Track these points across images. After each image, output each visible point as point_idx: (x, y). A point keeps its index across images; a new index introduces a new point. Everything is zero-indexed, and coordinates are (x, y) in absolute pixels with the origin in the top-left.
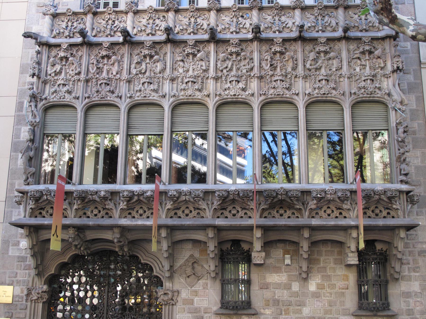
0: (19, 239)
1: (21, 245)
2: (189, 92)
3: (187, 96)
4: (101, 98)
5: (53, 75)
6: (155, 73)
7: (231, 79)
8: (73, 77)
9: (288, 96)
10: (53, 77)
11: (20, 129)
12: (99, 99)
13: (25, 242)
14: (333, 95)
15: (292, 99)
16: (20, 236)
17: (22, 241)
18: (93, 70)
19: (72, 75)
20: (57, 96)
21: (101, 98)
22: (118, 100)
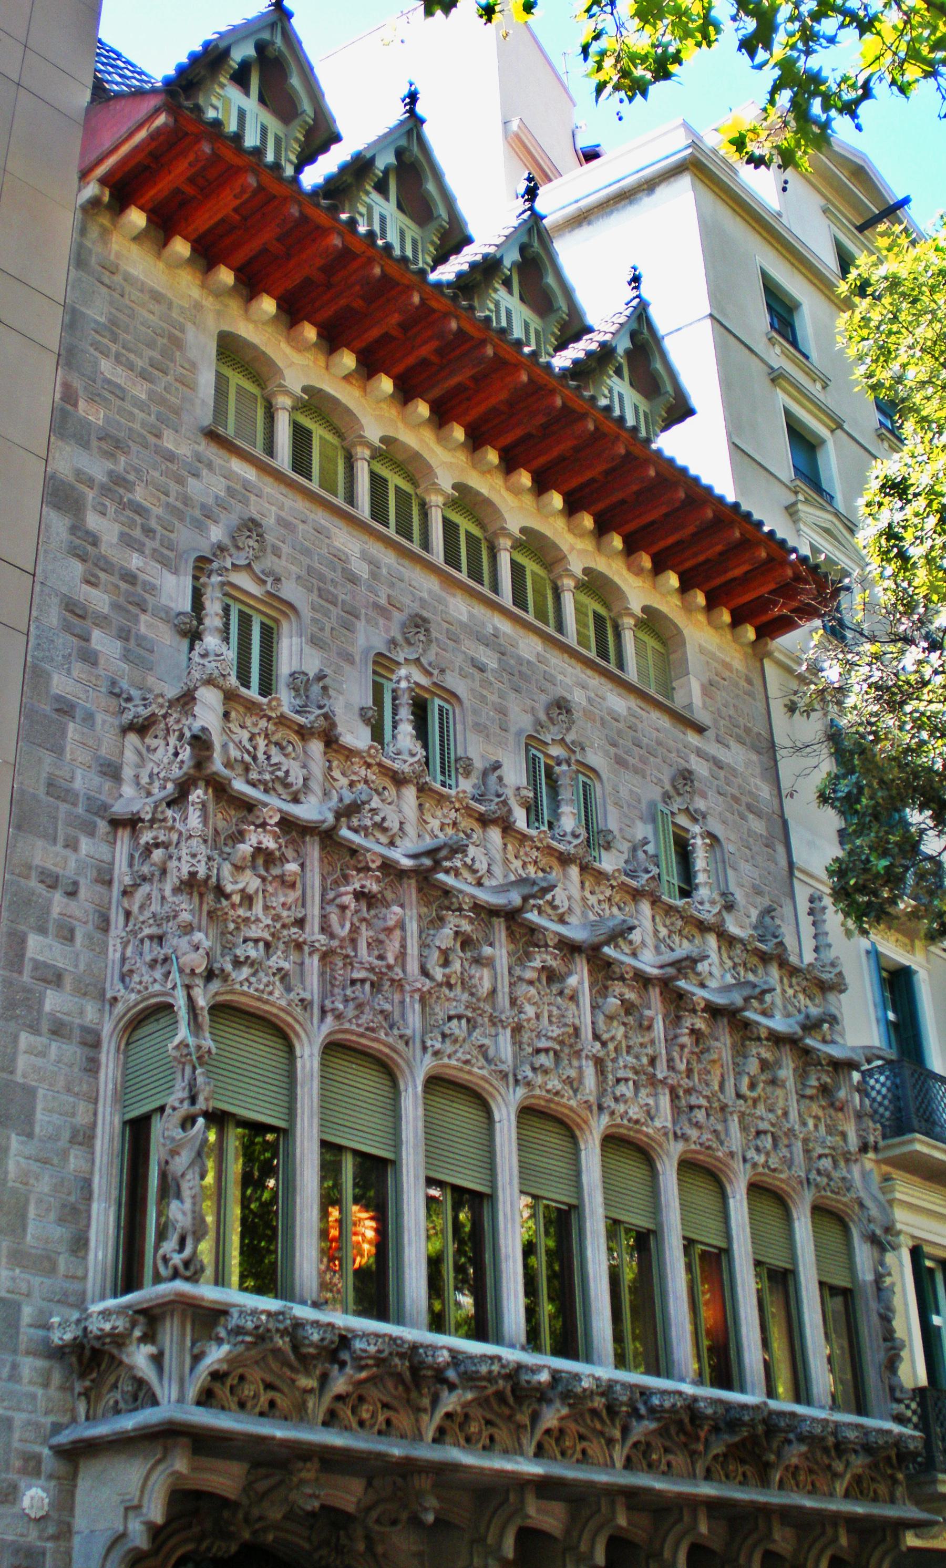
0: (15, 1477)
1: (26, 1502)
2: (554, 1083)
3: (548, 1091)
4: (367, 1029)
5: (236, 898)
6: (472, 994)
7: (621, 1074)
8: (284, 926)
9: (720, 1154)
10: (233, 906)
11: (16, 1038)
12: (361, 1030)
13: (40, 1491)
14: (782, 1176)
15: (727, 1165)
16: (18, 1463)
17: (30, 1487)
18: (343, 926)
19: (287, 921)
20: (253, 979)
21: (367, 1029)
22: (400, 1046)
